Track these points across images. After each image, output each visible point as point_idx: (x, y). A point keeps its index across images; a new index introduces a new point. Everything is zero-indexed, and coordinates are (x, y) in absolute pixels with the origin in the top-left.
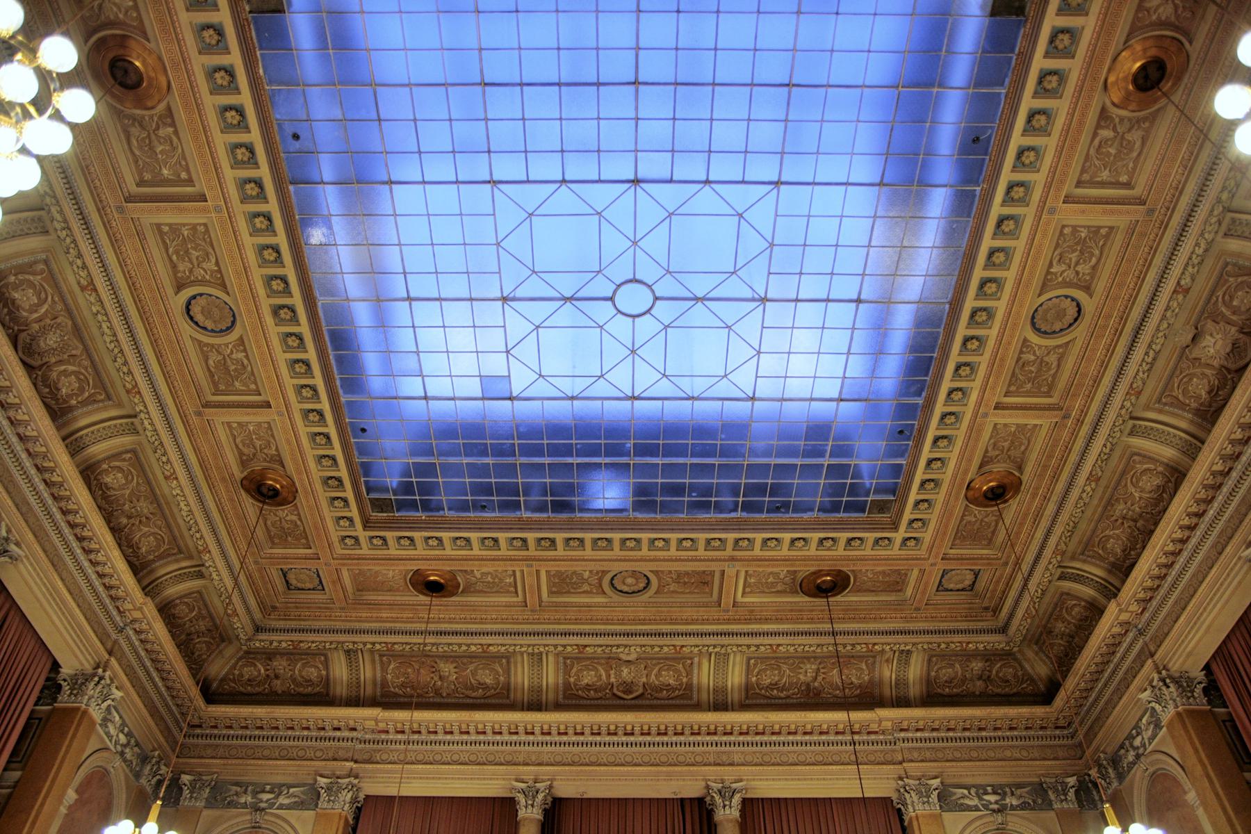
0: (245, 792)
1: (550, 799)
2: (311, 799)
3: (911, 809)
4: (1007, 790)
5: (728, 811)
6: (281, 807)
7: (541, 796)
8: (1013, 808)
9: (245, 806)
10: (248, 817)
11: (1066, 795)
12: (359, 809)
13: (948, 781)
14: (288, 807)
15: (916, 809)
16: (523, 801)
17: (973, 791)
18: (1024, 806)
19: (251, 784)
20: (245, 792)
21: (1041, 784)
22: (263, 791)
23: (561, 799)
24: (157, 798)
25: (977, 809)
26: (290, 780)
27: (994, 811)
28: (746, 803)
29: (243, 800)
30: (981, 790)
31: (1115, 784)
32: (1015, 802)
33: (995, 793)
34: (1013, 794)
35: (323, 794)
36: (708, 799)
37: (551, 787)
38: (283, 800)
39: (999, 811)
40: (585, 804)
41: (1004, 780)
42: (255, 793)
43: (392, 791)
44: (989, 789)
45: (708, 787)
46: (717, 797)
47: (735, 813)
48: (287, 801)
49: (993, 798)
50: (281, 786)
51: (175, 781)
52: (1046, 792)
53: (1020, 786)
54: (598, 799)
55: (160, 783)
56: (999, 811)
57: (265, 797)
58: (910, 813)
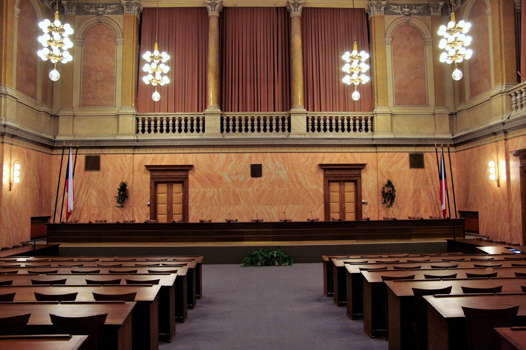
0: (91, 8)
1: (221, 8)
2: (120, 10)
3: (372, 13)
4: (414, 7)
5: (296, 13)
6: (108, 13)
7: (217, 6)
8: (414, 14)
9: (93, 13)
10: (95, 18)
11: (437, 9)
12: (141, 14)
13: (390, 2)
14: (112, 13)
15: (374, 13)
16: (210, 9)
17: (399, 7)
18: (418, 14)
19: (93, 4)
20: (91, 8)
21: (428, 5)
22: (99, 7)
23: (226, 7)
24: (54, 11)
25: (399, 14)
26: (110, 2)
27: (406, 15)
28: (303, 9)
29: (91, 11)
30: (403, 6)
31: (459, 5)
32: (416, 12)
33: (408, 8)
34: (415, 8)
35: (125, 8)
36: (288, 7)
37: (222, 2)
38: (108, 11)
39: (408, 15)
40: (237, 10)
41: (413, 2)
42: (96, 8)
43: (154, 5)
44: (406, 6)
45: (288, 2)
46: (292, 7)
47: (299, 13)
48: (110, 11)
49: (406, 10)
50: (106, 4)
51: (60, 3)
52: (429, 8)
53: (419, 5)
54: (242, 7)
55: (53, 5)
56: (408, 15)
57: (101, 9)
58: (371, 15)
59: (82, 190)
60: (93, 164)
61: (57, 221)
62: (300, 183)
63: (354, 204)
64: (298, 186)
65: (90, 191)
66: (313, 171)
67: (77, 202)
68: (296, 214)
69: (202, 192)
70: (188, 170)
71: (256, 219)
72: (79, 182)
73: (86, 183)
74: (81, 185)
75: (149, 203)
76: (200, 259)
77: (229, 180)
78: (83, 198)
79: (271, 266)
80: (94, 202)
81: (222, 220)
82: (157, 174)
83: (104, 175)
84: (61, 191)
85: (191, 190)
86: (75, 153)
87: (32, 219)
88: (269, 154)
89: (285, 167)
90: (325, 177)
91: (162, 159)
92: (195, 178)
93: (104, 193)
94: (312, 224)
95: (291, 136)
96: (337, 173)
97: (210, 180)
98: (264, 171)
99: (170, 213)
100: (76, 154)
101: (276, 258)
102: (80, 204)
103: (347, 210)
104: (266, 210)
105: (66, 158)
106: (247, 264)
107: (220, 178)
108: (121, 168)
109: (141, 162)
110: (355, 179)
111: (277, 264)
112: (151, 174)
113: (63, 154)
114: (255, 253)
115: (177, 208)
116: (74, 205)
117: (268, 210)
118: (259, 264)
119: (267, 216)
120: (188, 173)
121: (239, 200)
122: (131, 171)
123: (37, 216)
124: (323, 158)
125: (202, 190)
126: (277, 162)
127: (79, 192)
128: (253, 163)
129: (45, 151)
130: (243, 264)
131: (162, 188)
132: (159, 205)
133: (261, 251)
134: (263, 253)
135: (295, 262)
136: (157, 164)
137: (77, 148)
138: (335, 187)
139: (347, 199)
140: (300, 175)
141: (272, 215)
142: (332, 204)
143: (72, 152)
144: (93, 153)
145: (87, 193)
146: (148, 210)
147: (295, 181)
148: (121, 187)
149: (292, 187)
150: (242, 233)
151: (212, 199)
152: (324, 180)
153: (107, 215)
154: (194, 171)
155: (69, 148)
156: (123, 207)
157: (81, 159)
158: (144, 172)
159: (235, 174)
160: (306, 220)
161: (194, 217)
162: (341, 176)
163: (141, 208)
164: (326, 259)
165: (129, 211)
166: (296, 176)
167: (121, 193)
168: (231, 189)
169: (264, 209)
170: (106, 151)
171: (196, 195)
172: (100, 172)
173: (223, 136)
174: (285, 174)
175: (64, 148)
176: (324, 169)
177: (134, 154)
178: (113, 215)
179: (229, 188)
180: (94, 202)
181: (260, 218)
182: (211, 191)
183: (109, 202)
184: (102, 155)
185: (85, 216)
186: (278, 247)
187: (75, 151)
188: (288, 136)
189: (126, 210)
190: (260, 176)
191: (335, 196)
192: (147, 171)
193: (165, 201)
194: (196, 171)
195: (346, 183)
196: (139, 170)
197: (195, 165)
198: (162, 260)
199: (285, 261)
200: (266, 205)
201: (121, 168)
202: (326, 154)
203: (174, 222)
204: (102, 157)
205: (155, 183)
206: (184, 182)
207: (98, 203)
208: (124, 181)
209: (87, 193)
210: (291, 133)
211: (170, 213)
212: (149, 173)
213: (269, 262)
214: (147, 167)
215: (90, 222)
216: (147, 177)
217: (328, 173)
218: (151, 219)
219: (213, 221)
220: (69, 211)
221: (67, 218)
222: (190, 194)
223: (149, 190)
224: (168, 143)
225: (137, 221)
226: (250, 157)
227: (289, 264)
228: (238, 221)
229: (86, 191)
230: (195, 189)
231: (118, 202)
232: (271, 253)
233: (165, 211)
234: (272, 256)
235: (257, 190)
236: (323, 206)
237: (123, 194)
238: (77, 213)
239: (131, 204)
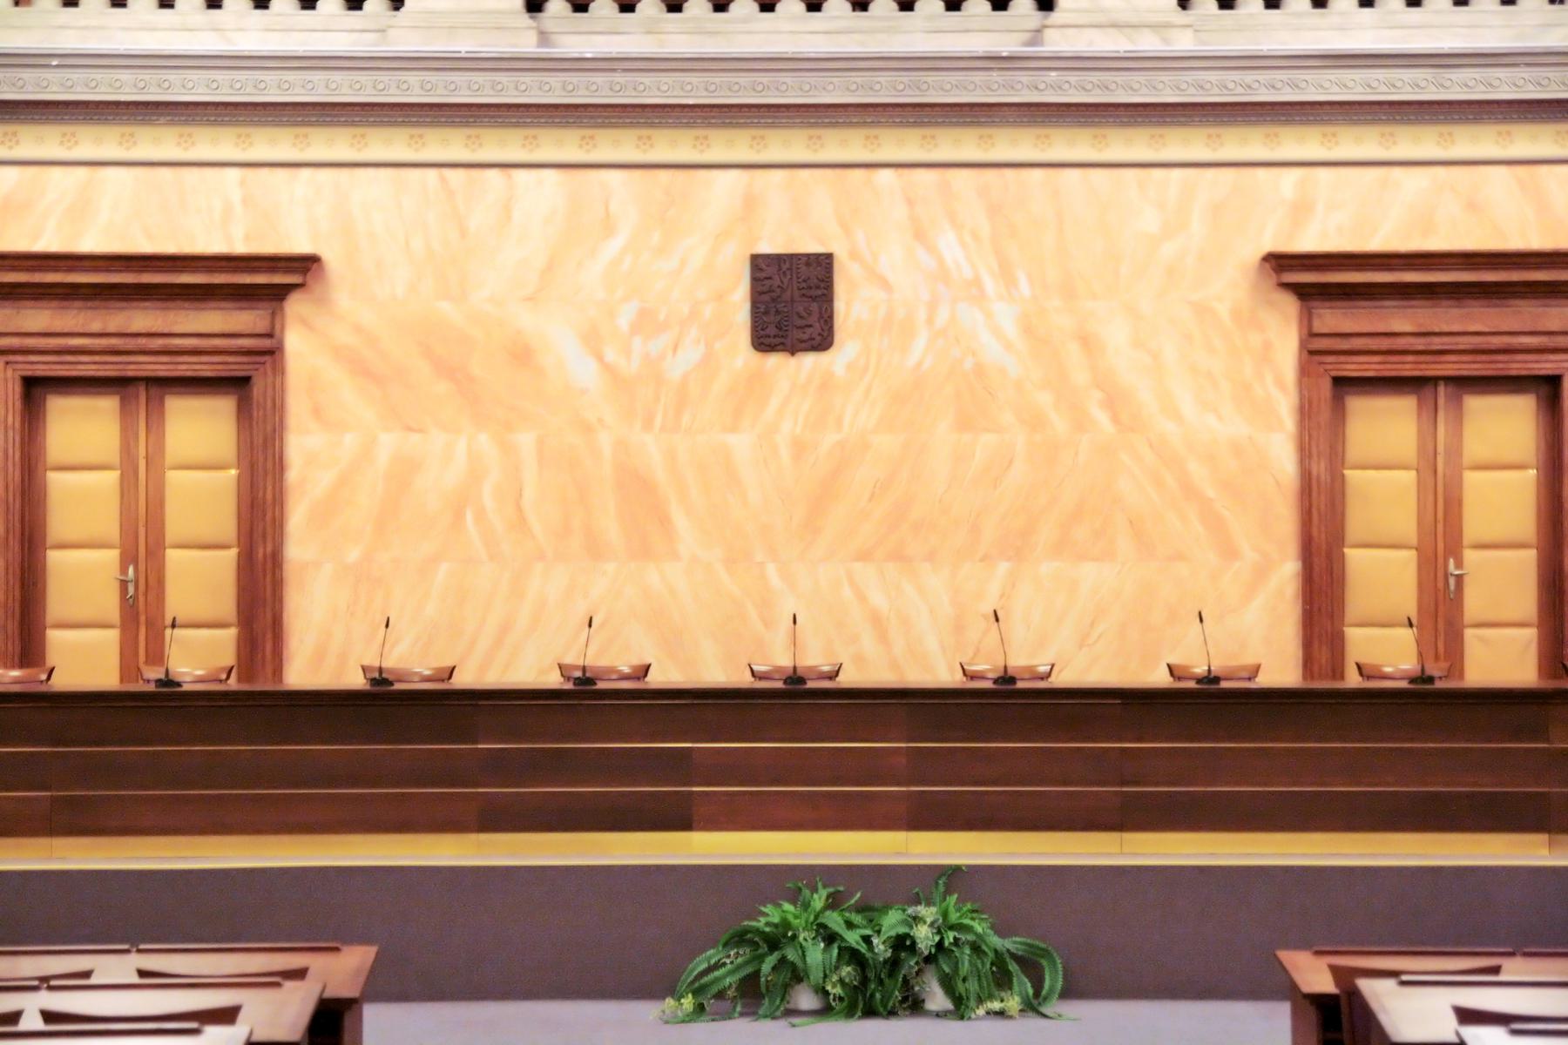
62: (1115, 401)
63: (1530, 557)
64: (1102, 418)
66: (1223, 310)
68: (1087, 634)
70: (279, 294)
71: (784, 660)
76: (340, 970)
77: (585, 372)
79: (892, 1013)
81: (533, 668)
88: (886, 175)
89: (1006, 274)
90: (1313, 352)
94: (1207, 706)
95: (1058, 41)
96: (1401, 320)
97: (450, 370)
98: (852, 303)
99: (142, 614)
101: (929, 959)
103: (1475, 603)
104: (861, 597)
106: (711, 1002)
107: (522, 355)
110: (1546, 366)
111: (937, 999)
114: (771, 915)
115: (200, 581)
117: (878, 599)
118: (806, 999)
119: (869, 644)
120: (276, 315)
121: (665, 521)
124: (1301, 210)
126: (949, 244)
128: (766, 248)
130: (688, 1002)
132: (54, 558)
133: (818, 902)
134: (834, 920)
135: (1069, 993)
138: (1384, 428)
139: (1475, 524)
140: (1116, 335)
141: (910, 635)
142: (1356, 558)
147: (1080, 376)
149: (1060, 424)
150: (679, 767)
151: (459, 515)
152: (1304, 371)
159: (636, 328)
160: (1159, 678)
161: (324, 651)
162: (1437, 343)
164: (1316, 977)
166: (1088, 342)
168: (605, 440)
169: (847, 593)
173: (544, 37)
174: (1011, 329)
176: (1304, 293)
179: (587, 429)
181: (814, 658)
182: (451, 454)
186: (954, 877)
188: (1037, 35)
190: (822, 340)
191: (1384, 496)
193: (107, 522)
195: (1478, 406)
198: (45, 982)
199: (1003, 981)
200: (864, 556)
202: (1322, 173)
203: (168, 682)
206: (245, 383)
210: (1055, 17)
211: (142, 614)
213: (879, 987)
217: (1332, 318)
219: (465, 679)
222: (293, 475)
224: (125, 86)
226: (750, 203)
227: (1032, 1007)
228: (656, 679)
232: (892, 922)
233: (109, 604)
234: (903, 944)
235: (799, 448)
236: (1288, 570)
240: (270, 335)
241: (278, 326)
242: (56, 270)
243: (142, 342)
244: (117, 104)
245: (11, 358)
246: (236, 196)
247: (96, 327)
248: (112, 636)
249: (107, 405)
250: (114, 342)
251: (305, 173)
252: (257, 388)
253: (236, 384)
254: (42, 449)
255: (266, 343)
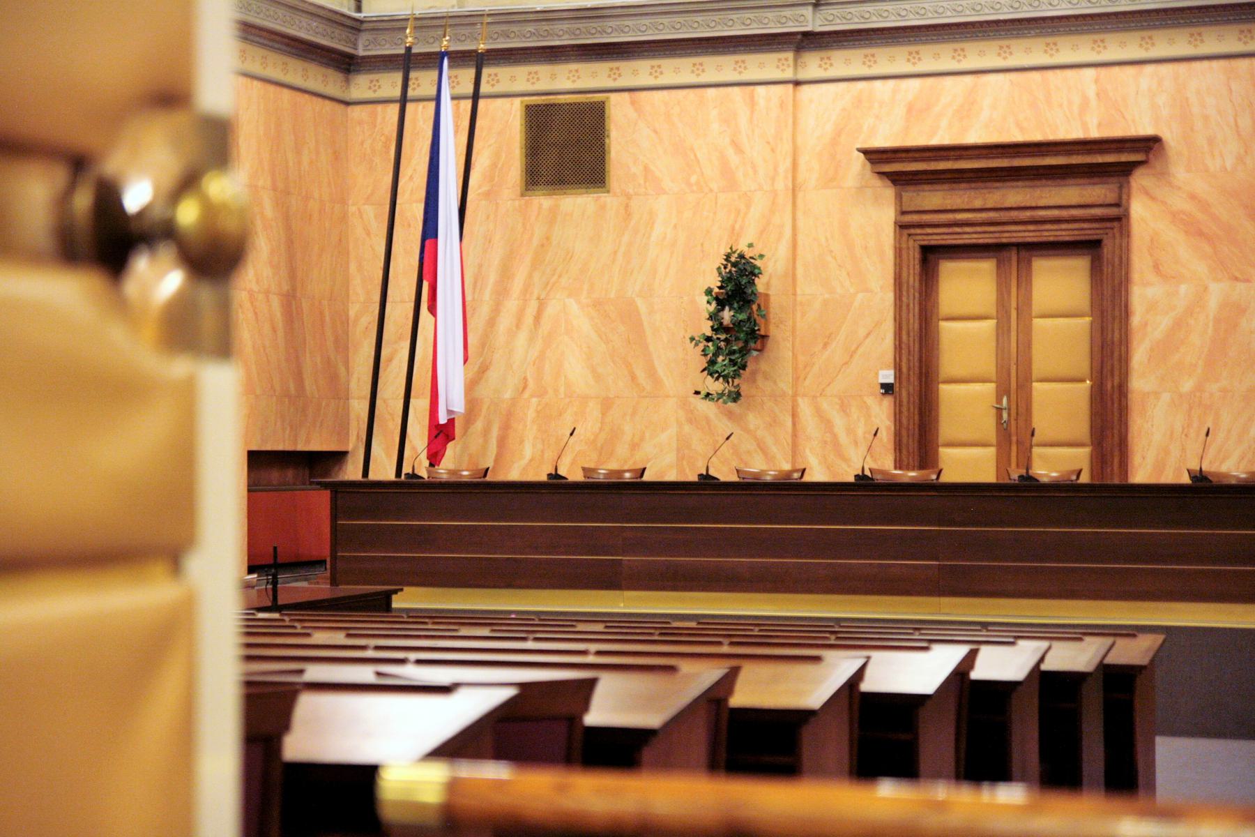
59: (511, 305)
60: (567, 150)
61: (384, 470)
65: (550, 311)
67: (484, 369)
69: (1213, 303)
70: (1125, 171)
72: (496, 256)
73: (536, 264)
74: (506, 273)
75: (888, 376)
78: (516, 354)
80: (576, 371)
82: (933, 198)
83: (628, 214)
84: (399, 312)
85: (1146, 295)
86: (470, 89)
87: (257, 460)
91: (966, 111)
92: (1176, 217)
93: (630, 316)
99: (1014, 431)
100: (476, 97)
102: (501, 385)
105: (420, 116)
108: (727, 172)
109: (838, 133)
112: (899, 198)
113: (403, 101)
115: (1060, 409)
116: (471, 386)
122: (782, 184)
123: (280, 447)
125: (1217, 291)
127: (496, 310)
129: (311, 85)
131: (967, 287)
132: (944, 389)
136: (935, 141)
137: (478, 60)
143: (458, 80)
144: (569, 85)
145: (537, 318)
146: (882, 413)
148: (726, 281)
153: (648, 448)
154: (1163, 175)
155: (433, 60)
156: (736, 397)
157: (504, 125)
158: (861, 189)
161: (1160, 454)
163: (844, 408)
165: (774, 423)
167: (727, 315)
170: (639, 71)
171: (1178, 324)
172: (604, 198)
175: (407, 62)
177: (797, 83)
178: (683, 445)
180: (576, 371)
183: (661, 372)
184: (614, 97)
185: (528, 452)
187: (466, 76)
189: (753, 420)
192: (877, 182)
193: (986, 362)
194: (1180, 172)
196: (830, 180)
197: (1166, 135)
201: (727, 172)
204: (619, 111)
205: (926, 256)
206: (1098, 245)
207: (598, 377)
208: (742, 247)
209: (537, 318)
211: (1014, 431)
212: (889, 192)
214: (875, 156)
215: (555, 476)
216: (875, 217)
218: (899, 464)
220: (443, 420)
221: (435, 457)
222: (1136, 320)
223: (890, 296)
225: (817, 474)
229: (533, 306)
230: (1171, 282)
231: (710, 368)
237: (739, 321)
238: (486, 432)
239: (785, 385)
240: (1117, 205)
241: (1124, 197)
242: (947, 159)
243: (1014, 214)
244: (997, 22)
245: (912, 231)
246: (1091, 91)
247: (978, 204)
248: (991, 451)
249: (985, 268)
250: (992, 215)
251: (1149, 69)
252: (1107, 250)
253: (1090, 247)
254: (936, 304)
255: (1113, 211)
